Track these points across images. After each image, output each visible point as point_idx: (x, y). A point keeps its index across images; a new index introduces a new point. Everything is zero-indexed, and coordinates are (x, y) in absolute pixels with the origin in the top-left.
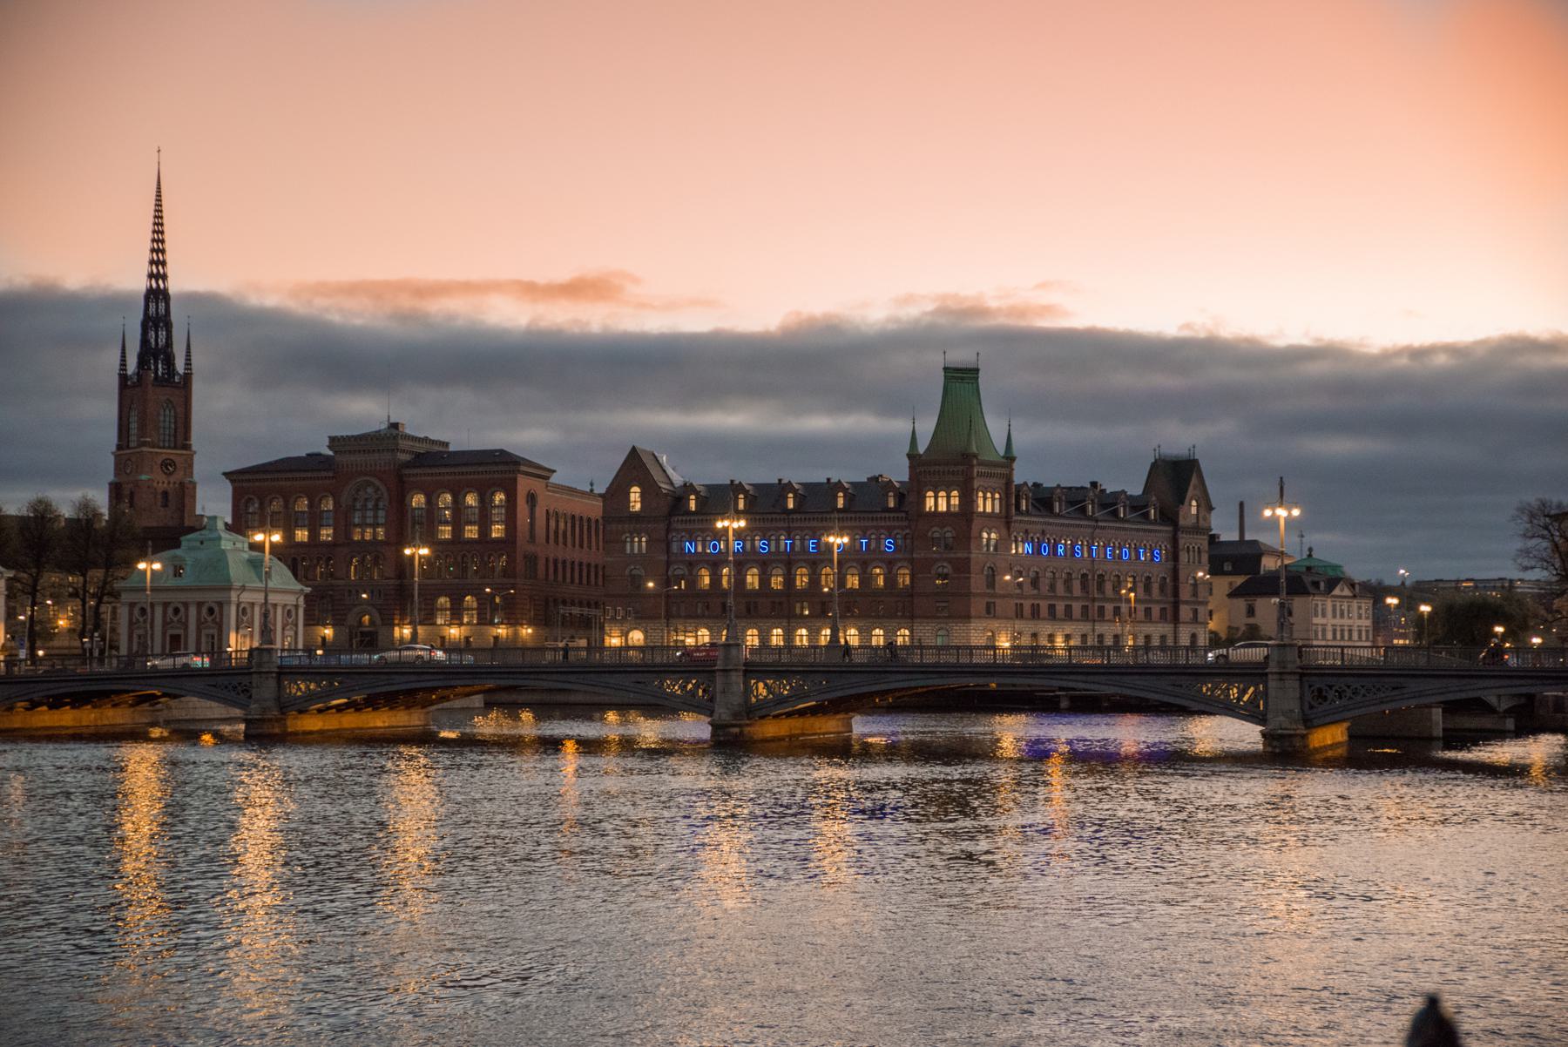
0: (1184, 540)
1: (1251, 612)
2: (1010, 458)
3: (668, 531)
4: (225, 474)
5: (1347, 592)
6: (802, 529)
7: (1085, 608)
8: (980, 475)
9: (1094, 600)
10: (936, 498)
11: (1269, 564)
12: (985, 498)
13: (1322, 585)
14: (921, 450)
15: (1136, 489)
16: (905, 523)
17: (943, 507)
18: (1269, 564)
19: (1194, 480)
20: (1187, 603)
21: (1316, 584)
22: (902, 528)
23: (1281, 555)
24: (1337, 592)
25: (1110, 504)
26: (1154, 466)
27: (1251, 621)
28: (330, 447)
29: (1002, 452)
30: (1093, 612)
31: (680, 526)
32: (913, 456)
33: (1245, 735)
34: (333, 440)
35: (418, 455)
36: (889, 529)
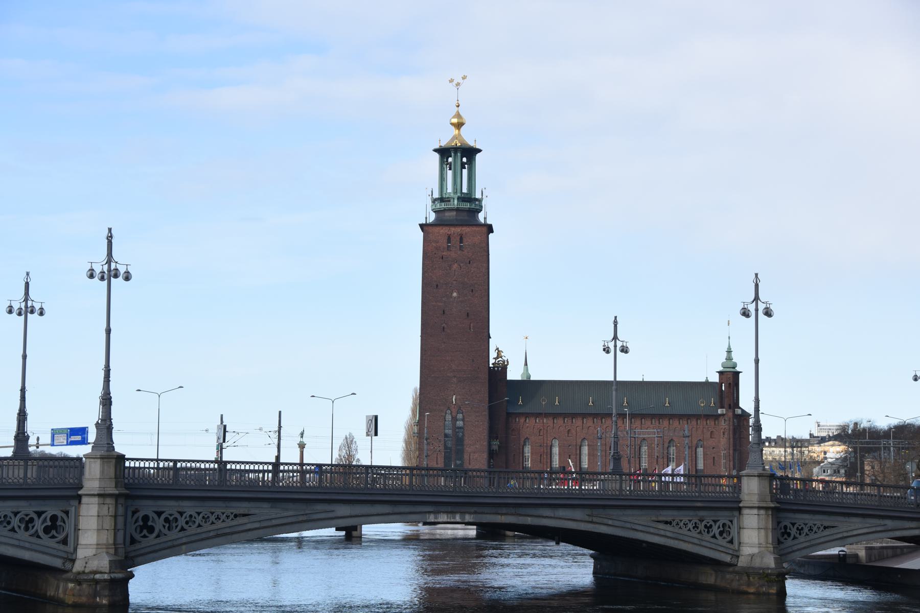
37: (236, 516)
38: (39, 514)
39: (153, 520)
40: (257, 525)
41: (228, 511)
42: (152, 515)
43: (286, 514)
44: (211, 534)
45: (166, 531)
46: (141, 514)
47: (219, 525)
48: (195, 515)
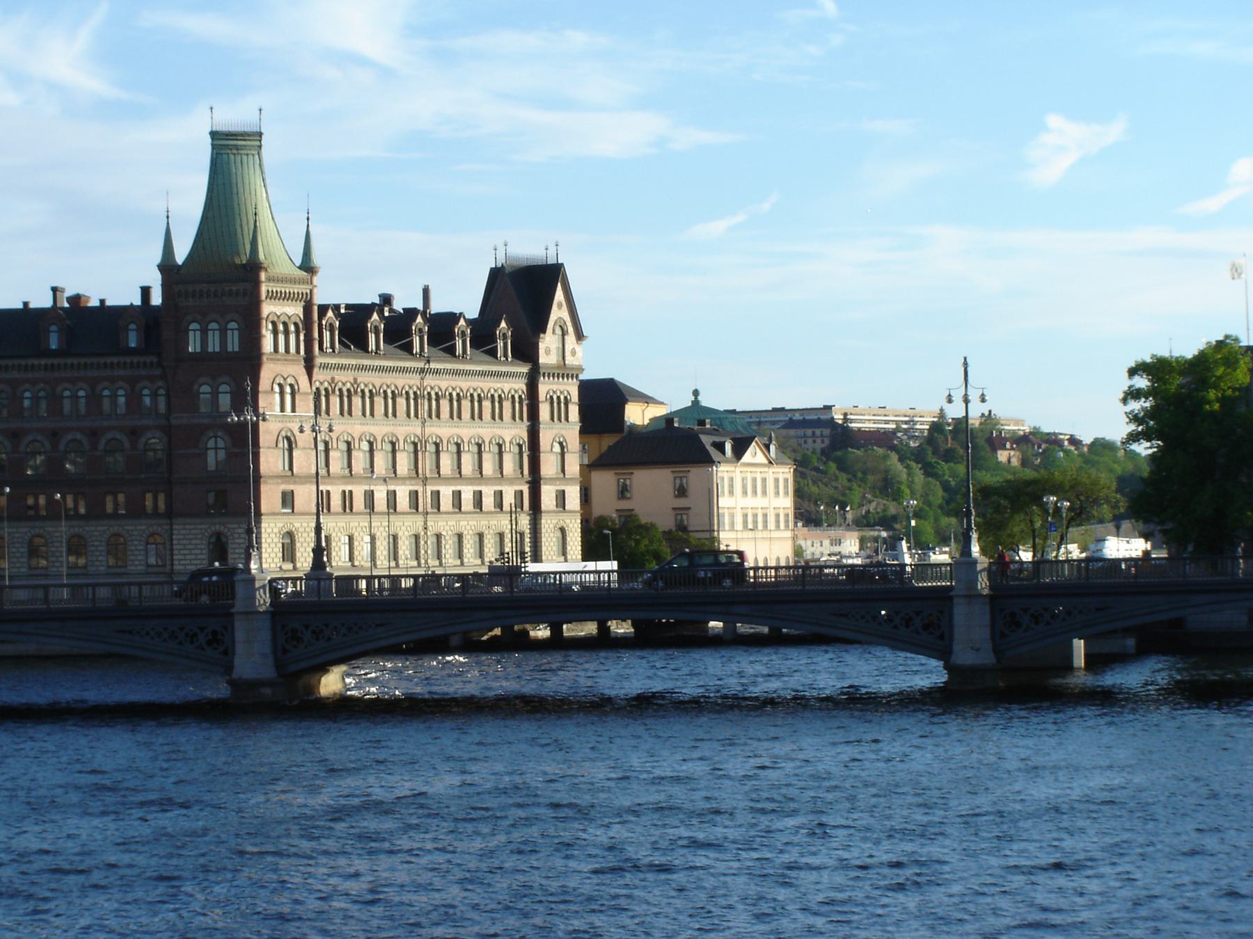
0: (544, 388)
1: (623, 492)
5: (761, 458)
7: (414, 496)
8: (272, 296)
9: (425, 481)
10: (204, 332)
11: (636, 415)
12: (275, 332)
13: (728, 447)
15: (470, 307)
16: (158, 372)
17: (214, 345)
18: (636, 415)
19: (559, 295)
20: (551, 481)
21: (720, 447)
23: (647, 399)
24: (747, 457)
25: (442, 330)
26: (496, 275)
27: (624, 505)
30: (425, 501)
32: (167, 267)
33: (928, 673)
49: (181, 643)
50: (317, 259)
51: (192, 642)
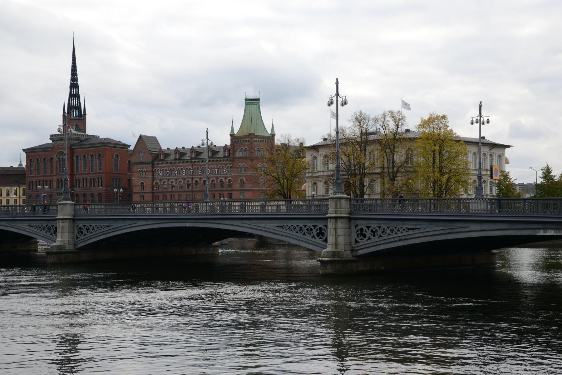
2: (273, 135)
3: (153, 167)
4: (24, 150)
6: (197, 165)
14: (236, 132)
22: (230, 164)
28: (50, 139)
29: (270, 132)
31: (157, 165)
32: (232, 135)
34: (51, 136)
35: (81, 141)
36: (226, 164)
37: (409, 229)
38: (315, 226)
39: (366, 231)
40: (421, 235)
41: (404, 227)
42: (365, 228)
43: (437, 229)
44: (396, 239)
45: (372, 237)
46: (359, 228)
47: (400, 234)
48: (386, 228)
49: (304, 234)
50: (276, 132)
51: (310, 234)
